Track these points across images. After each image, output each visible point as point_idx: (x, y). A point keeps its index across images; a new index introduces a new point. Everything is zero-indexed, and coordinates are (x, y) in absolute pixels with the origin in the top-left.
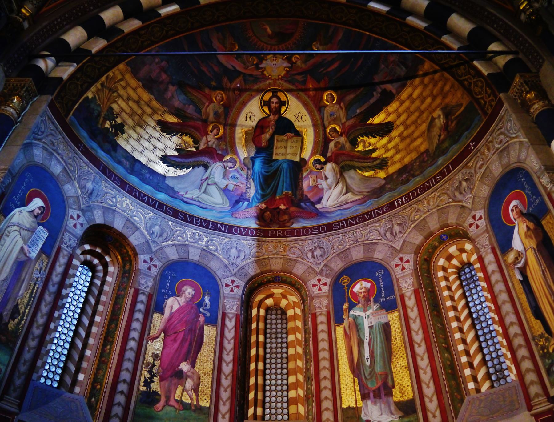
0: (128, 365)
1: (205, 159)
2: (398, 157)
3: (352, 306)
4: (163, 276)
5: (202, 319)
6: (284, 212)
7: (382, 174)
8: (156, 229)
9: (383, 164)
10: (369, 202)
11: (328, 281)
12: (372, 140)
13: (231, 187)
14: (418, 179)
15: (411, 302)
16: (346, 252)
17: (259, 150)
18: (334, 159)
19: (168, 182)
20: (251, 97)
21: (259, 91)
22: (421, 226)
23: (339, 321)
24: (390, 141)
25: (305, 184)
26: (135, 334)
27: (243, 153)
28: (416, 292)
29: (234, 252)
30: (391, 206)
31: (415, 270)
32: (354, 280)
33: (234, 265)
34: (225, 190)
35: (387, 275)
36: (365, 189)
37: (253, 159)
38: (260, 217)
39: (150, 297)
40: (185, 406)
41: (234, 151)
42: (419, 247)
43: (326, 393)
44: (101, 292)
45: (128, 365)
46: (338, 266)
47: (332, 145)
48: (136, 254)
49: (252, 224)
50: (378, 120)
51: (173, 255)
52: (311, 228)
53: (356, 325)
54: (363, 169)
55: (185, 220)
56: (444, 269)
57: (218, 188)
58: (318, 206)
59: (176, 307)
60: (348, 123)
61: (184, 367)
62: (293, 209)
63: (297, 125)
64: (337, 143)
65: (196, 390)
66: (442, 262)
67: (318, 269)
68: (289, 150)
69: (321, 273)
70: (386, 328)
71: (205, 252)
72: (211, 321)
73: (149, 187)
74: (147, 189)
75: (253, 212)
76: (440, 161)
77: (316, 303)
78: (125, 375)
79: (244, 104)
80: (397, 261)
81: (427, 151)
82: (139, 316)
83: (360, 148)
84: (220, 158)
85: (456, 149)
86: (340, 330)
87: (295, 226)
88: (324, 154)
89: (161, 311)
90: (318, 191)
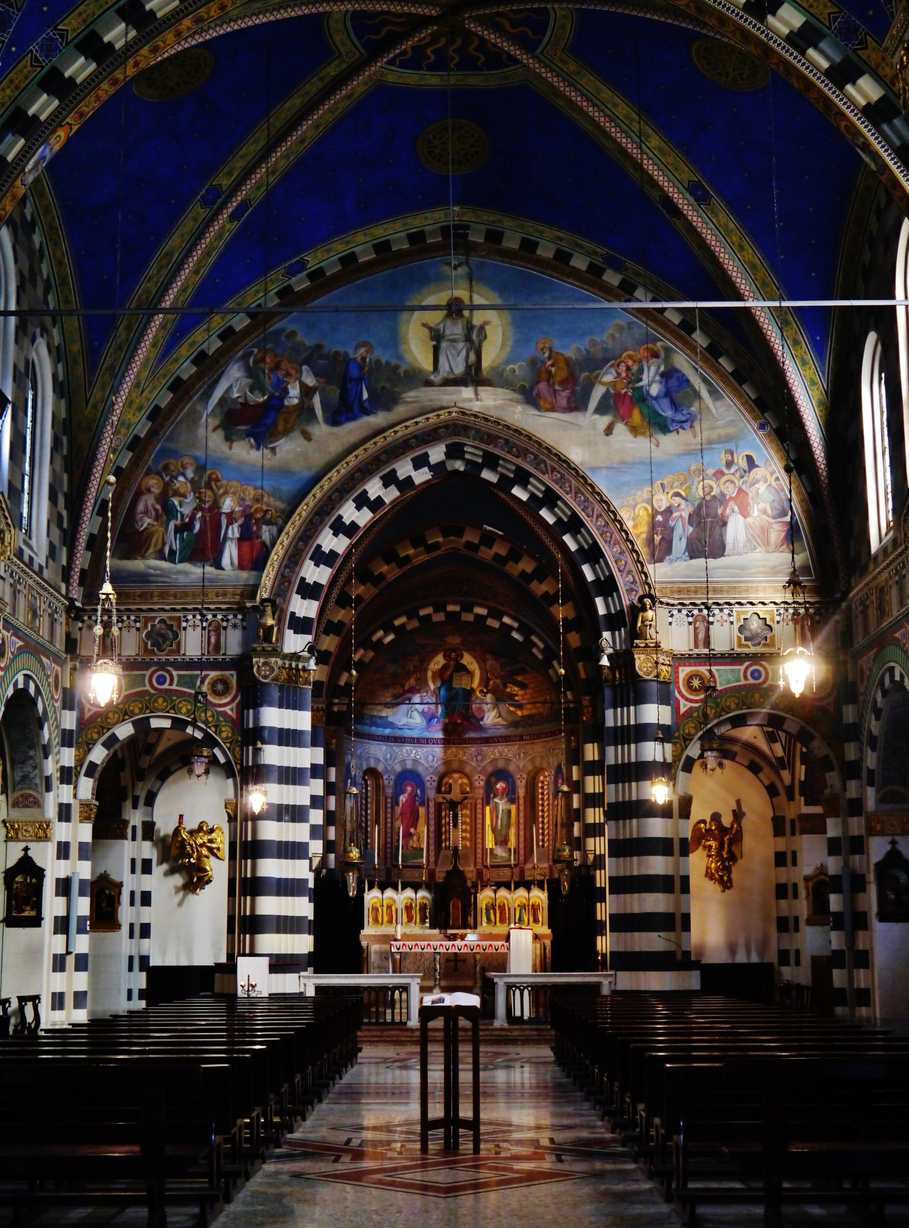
0: (389, 835)
1: (409, 695)
2: (529, 706)
3: (495, 796)
4: (396, 784)
5: (417, 803)
6: (461, 724)
7: (519, 713)
8: (389, 755)
10: (511, 729)
11: (484, 778)
12: (516, 689)
13: (426, 710)
14: (536, 728)
15: (521, 802)
16: (494, 761)
17: (444, 682)
18: (492, 691)
19: (390, 719)
20: (437, 654)
21: (442, 650)
22: (532, 760)
23: (488, 804)
24: (526, 694)
25: (474, 706)
26: (389, 820)
27: (432, 687)
28: (525, 798)
29: (430, 758)
30: (521, 738)
31: (526, 785)
32: (496, 784)
33: (432, 767)
34: (423, 713)
35: (514, 783)
36: (510, 719)
37: (439, 689)
38: (445, 729)
39: (392, 799)
40: (415, 849)
41: (427, 684)
42: (530, 772)
43: (479, 841)
44: (367, 797)
45: (389, 835)
46: (490, 769)
47: (491, 682)
48: (382, 777)
49: (440, 735)
50: (519, 678)
51: (398, 769)
52: (477, 739)
53: (496, 807)
54: (510, 705)
55: (402, 742)
56: (543, 782)
57: (419, 712)
58: (481, 723)
59: (404, 800)
60: (502, 673)
61: (412, 830)
62: (465, 723)
63: (470, 667)
64: (494, 683)
65: (418, 840)
66: (542, 778)
67: (479, 769)
68: (463, 682)
69: (480, 772)
70: (509, 812)
71: (415, 761)
72: (422, 804)
73: (380, 729)
74: (379, 731)
75: (439, 726)
76: (546, 726)
77: (477, 791)
78: (389, 840)
79: (433, 657)
80: (519, 776)
81: (540, 714)
82: (389, 810)
83: (508, 690)
84: (419, 691)
86: (488, 809)
87: (467, 736)
88: (486, 686)
89: (398, 805)
90: (483, 712)
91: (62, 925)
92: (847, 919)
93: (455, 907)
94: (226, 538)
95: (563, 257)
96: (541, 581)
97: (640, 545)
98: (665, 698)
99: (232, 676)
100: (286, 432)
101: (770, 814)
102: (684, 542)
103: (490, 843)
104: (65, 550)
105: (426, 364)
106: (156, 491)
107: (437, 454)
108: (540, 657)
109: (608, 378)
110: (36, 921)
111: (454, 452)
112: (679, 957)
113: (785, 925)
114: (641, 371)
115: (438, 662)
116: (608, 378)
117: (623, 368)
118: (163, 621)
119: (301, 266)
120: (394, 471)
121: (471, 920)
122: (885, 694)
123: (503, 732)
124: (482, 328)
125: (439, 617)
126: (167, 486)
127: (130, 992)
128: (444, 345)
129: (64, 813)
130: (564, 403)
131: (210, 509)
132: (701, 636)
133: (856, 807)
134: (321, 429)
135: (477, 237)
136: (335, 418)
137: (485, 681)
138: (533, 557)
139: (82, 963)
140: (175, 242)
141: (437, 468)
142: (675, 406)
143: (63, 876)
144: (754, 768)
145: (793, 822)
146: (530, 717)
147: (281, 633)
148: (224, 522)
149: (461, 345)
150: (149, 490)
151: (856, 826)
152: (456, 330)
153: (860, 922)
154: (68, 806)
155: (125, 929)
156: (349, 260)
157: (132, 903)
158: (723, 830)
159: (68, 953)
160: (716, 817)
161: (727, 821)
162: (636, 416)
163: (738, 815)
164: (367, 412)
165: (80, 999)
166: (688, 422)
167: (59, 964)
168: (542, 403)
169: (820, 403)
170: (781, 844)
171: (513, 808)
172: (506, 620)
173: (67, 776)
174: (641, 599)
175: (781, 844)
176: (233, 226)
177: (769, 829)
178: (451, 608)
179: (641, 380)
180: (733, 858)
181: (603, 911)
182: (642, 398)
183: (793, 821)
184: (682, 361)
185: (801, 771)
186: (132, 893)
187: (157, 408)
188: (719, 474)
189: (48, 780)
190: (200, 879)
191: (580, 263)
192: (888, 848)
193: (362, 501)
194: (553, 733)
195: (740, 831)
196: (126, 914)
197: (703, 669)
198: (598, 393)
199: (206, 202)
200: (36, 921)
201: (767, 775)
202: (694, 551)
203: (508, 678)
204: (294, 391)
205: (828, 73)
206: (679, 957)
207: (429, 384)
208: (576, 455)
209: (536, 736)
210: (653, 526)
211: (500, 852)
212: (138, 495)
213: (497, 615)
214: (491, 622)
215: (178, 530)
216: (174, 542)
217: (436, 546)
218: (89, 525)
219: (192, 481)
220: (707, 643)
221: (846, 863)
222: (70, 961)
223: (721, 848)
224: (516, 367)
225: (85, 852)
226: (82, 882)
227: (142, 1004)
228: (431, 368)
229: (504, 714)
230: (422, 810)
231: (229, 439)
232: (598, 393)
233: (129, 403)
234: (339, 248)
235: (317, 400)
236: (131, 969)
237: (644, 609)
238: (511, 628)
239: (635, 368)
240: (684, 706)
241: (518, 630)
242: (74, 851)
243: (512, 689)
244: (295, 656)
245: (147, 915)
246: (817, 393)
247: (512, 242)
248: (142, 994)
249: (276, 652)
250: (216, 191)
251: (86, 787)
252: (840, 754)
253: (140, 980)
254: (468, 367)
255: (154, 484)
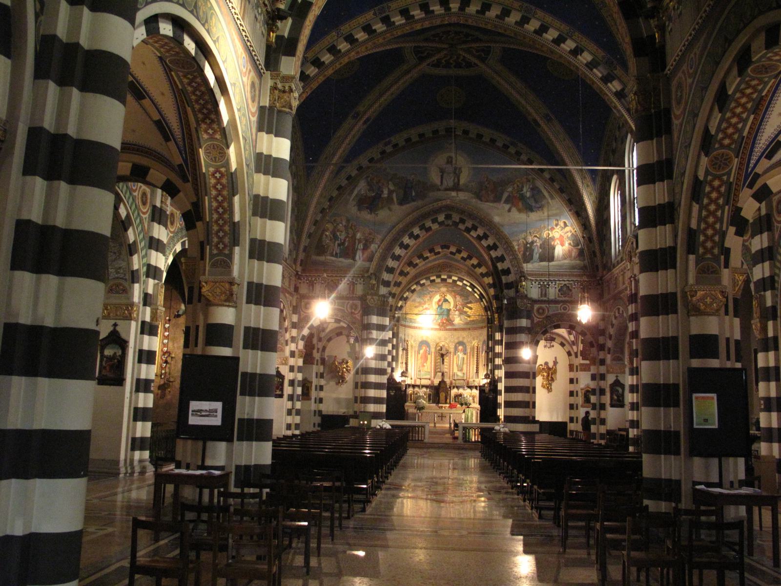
9: (469, 316)
17: (439, 306)
18: (459, 310)
30: (469, 329)
46: (456, 341)
50: (469, 305)
51: (420, 340)
53: (458, 356)
85: (481, 325)
86: (455, 357)
91: (291, 398)
92: (598, 406)
93: (442, 395)
94: (357, 249)
95: (493, 141)
96: (480, 268)
97: (520, 256)
98: (529, 317)
99: (358, 303)
100: (382, 208)
101: (568, 363)
102: (538, 255)
103: (455, 370)
104: (295, 252)
105: (438, 182)
106: (331, 229)
107: (441, 218)
108: (478, 297)
109: (510, 189)
110: (281, 396)
111: (448, 217)
112: (531, 418)
113: (571, 407)
114: (523, 187)
115: (437, 298)
116: (510, 189)
117: (515, 185)
118: (332, 281)
119: (389, 143)
120: (424, 224)
121: (448, 401)
122: (616, 318)
123: (462, 326)
124: (460, 168)
125: (439, 280)
126: (335, 227)
127: (314, 424)
128: (445, 175)
129: (293, 354)
130: (492, 199)
131: (352, 237)
132: (544, 293)
133: (602, 362)
134: (396, 207)
135: (459, 133)
136: (401, 203)
137: (456, 306)
138: (477, 258)
139: (298, 412)
140: (340, 133)
141: (441, 224)
142: (536, 202)
143: (291, 378)
144: (562, 345)
145: (577, 366)
146: (473, 321)
147: (378, 287)
148: (357, 241)
149: (451, 175)
150: (328, 229)
151: (603, 369)
152: (449, 168)
153: (603, 407)
154: (294, 352)
155: (313, 400)
156: (408, 140)
157: (316, 390)
158: (549, 369)
159: (293, 408)
160: (546, 363)
161: (551, 365)
162: (520, 204)
163: (555, 363)
164: (414, 201)
165: (297, 426)
166: (541, 208)
167: (289, 412)
168: (483, 199)
169: (594, 202)
170: (573, 375)
171: (465, 356)
172: (465, 282)
173: (293, 339)
174: (521, 277)
175: (573, 375)
176: (365, 127)
177: (568, 369)
178: (443, 277)
179: (522, 190)
180: (553, 380)
181: (501, 399)
182: (522, 198)
183: (577, 366)
184: (540, 184)
185: (581, 347)
186: (316, 386)
187: (332, 197)
188: (553, 229)
189: (287, 341)
190: (343, 381)
191: (499, 144)
192: (615, 378)
193: (411, 236)
194: (482, 328)
195: (556, 370)
196: (314, 394)
197: (543, 306)
198: (505, 195)
199: (354, 117)
200: (281, 396)
201: (567, 347)
202: (542, 259)
203: (465, 305)
204: (386, 192)
205: (601, 79)
206: (531, 418)
207: (439, 190)
208: (497, 219)
209: (475, 329)
210: (526, 249)
211: (460, 374)
212: (324, 231)
213: (461, 280)
214: (459, 283)
215: (339, 245)
216: (337, 250)
217: (439, 253)
218: (305, 241)
219: (345, 226)
220: (545, 295)
221: (598, 384)
222: (294, 412)
223: (548, 376)
224: (473, 184)
225: (300, 369)
226: (299, 381)
227: (319, 429)
228: (439, 183)
229: (463, 318)
230: (429, 356)
231: (359, 210)
232: (505, 195)
233: (321, 195)
234: (405, 135)
235: (394, 195)
236: (315, 415)
237: (521, 281)
238: (467, 285)
239: (520, 186)
240: (536, 320)
241: (469, 287)
242: (296, 369)
243: (466, 309)
244: (384, 296)
245: (322, 394)
246: (593, 198)
247: (472, 135)
248: (319, 425)
249: (376, 294)
250: (358, 114)
251: (301, 345)
252: (597, 342)
253: (318, 420)
254: (455, 184)
255: (330, 226)
